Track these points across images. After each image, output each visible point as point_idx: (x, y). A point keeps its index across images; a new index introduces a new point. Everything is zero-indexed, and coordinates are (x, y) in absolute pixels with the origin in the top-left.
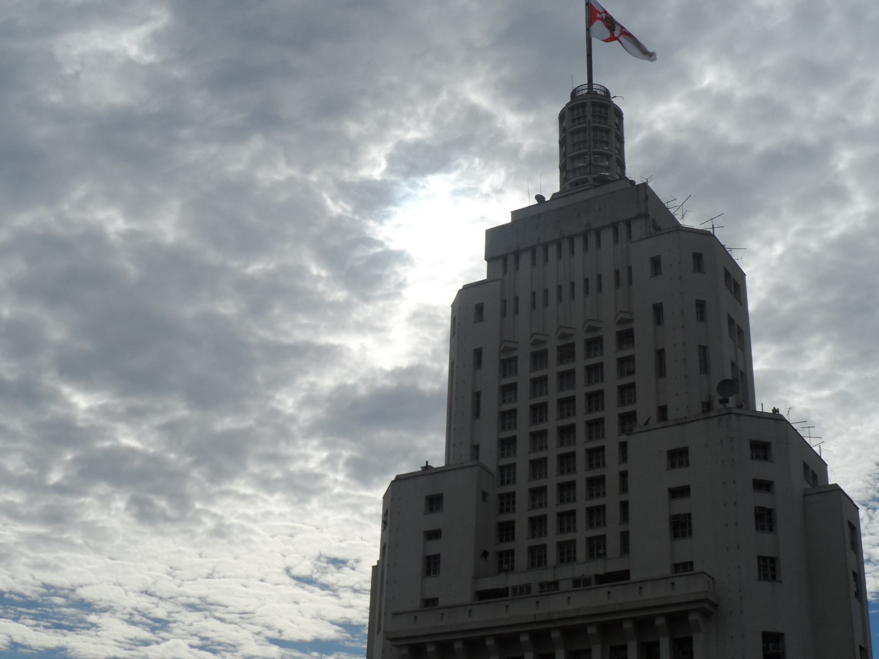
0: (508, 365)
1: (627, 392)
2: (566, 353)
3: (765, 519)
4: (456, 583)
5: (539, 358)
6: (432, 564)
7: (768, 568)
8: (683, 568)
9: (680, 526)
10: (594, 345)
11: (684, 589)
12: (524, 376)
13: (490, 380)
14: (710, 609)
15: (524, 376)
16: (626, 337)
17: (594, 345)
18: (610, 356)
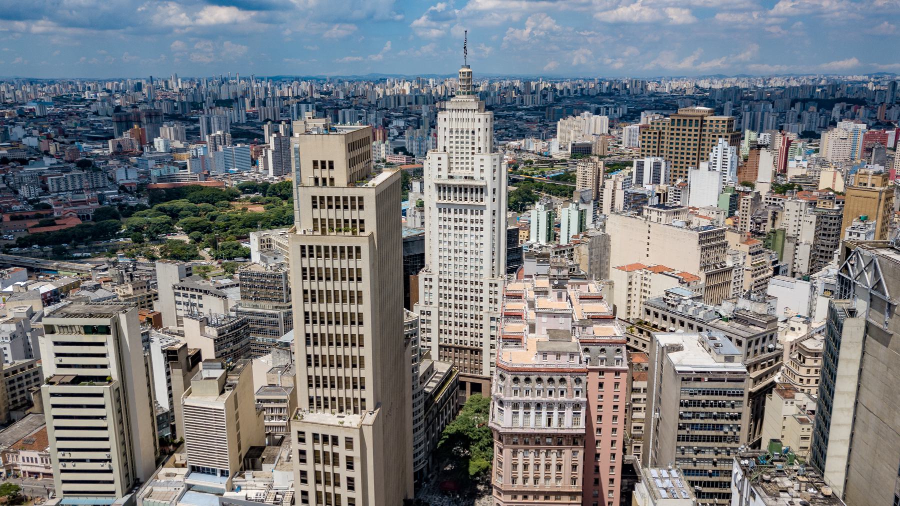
0: (451, 131)
1: (473, 143)
2: (462, 132)
3: (494, 171)
4: (444, 173)
5: (457, 131)
6: (440, 169)
7: (494, 178)
8: (482, 178)
9: (482, 171)
10: (467, 132)
11: (483, 183)
12: (454, 135)
13: (447, 134)
14: (486, 186)
15: (454, 135)
16: (473, 133)
17: (467, 132)
18: (470, 135)
